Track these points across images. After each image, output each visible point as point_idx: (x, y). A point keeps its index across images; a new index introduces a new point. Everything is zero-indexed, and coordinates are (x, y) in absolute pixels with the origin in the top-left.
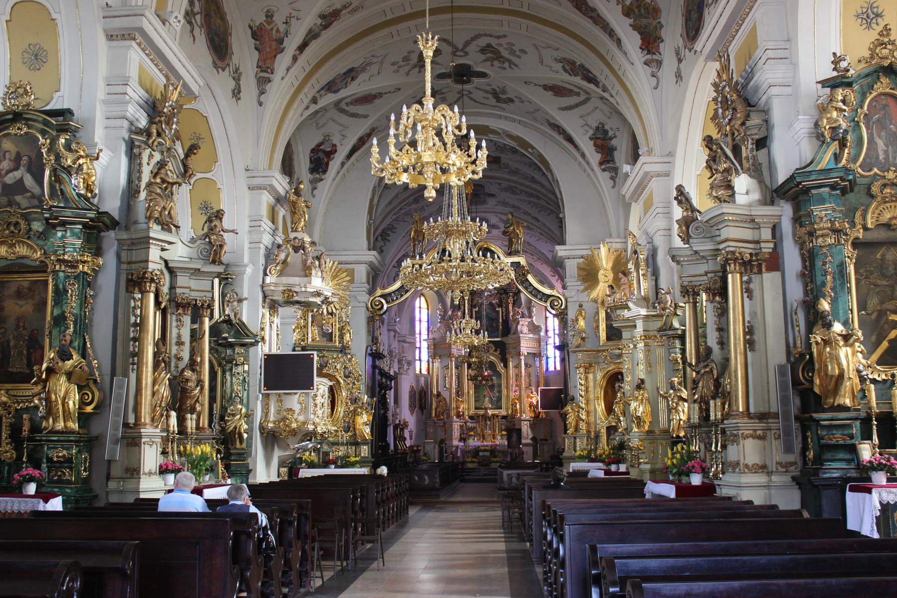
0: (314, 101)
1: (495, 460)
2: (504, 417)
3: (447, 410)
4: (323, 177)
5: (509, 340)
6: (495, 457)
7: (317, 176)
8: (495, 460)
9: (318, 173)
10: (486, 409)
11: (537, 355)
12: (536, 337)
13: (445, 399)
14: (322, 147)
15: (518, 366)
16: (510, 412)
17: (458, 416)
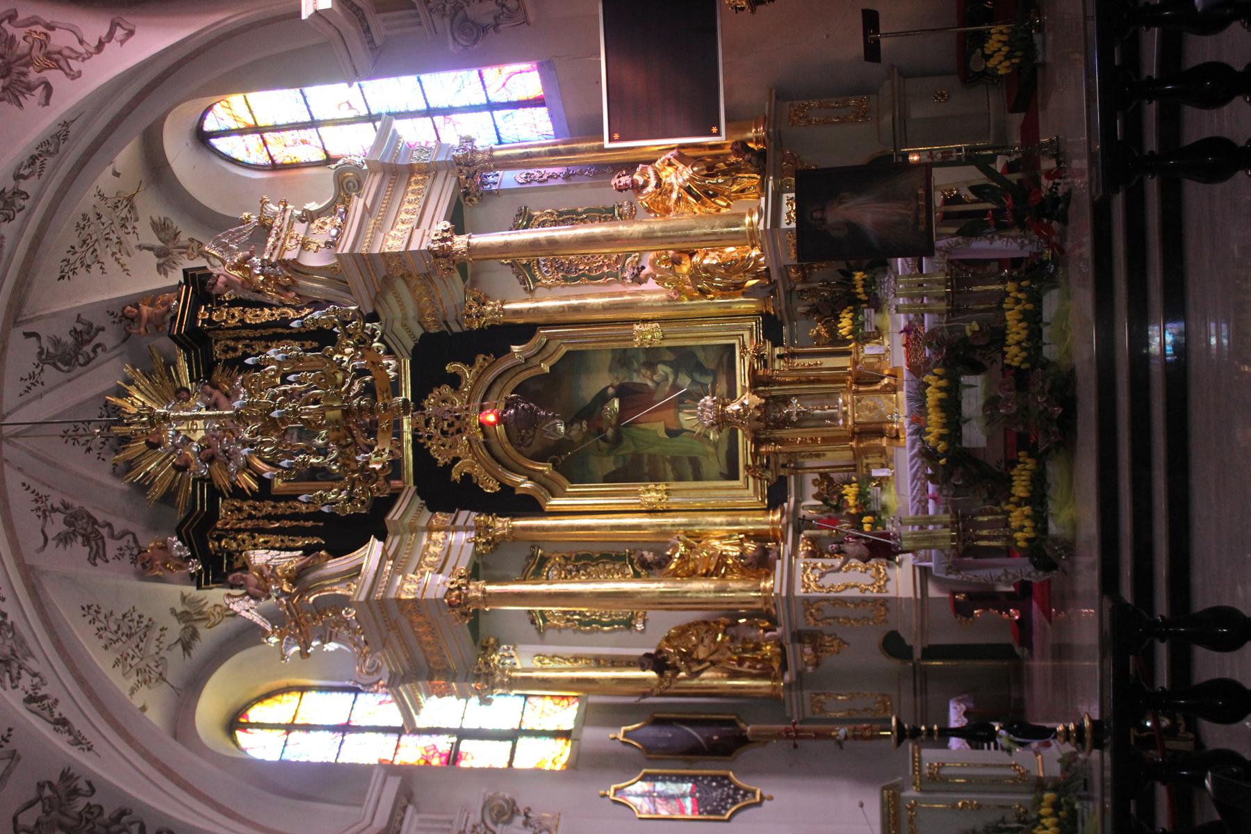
1: (1016, 331)
2: (772, 328)
3: (727, 617)
5: (406, 315)
6: (998, 336)
8: (1016, 331)
10: (722, 421)
11: (469, 183)
12: (372, 184)
13: (683, 631)
15: (525, 265)
16: (743, 304)
17: (761, 564)
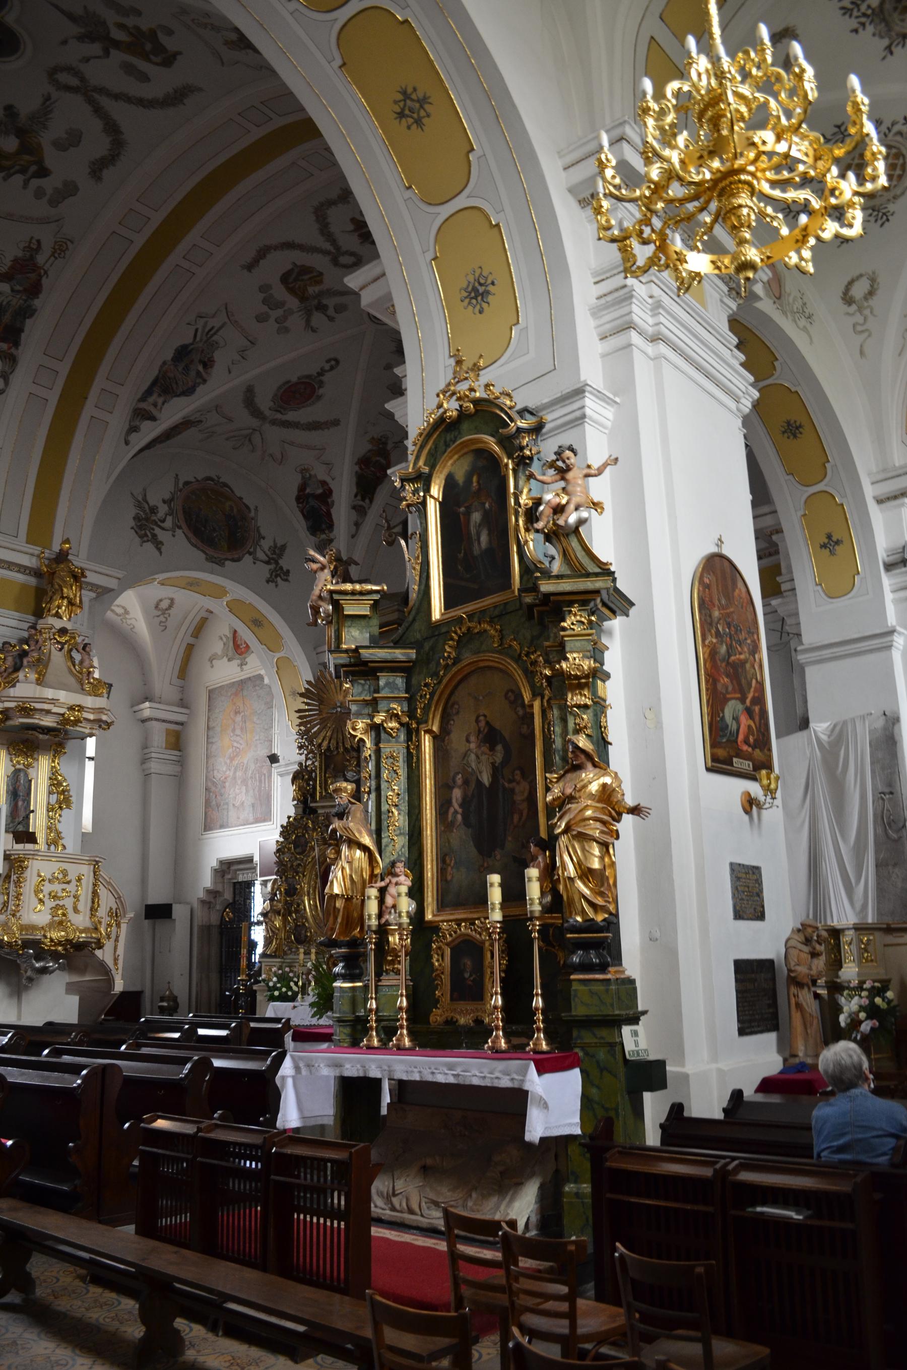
0: (142, 415)
4: (332, 536)
7: (323, 536)
9: (323, 532)
14: (308, 491)
